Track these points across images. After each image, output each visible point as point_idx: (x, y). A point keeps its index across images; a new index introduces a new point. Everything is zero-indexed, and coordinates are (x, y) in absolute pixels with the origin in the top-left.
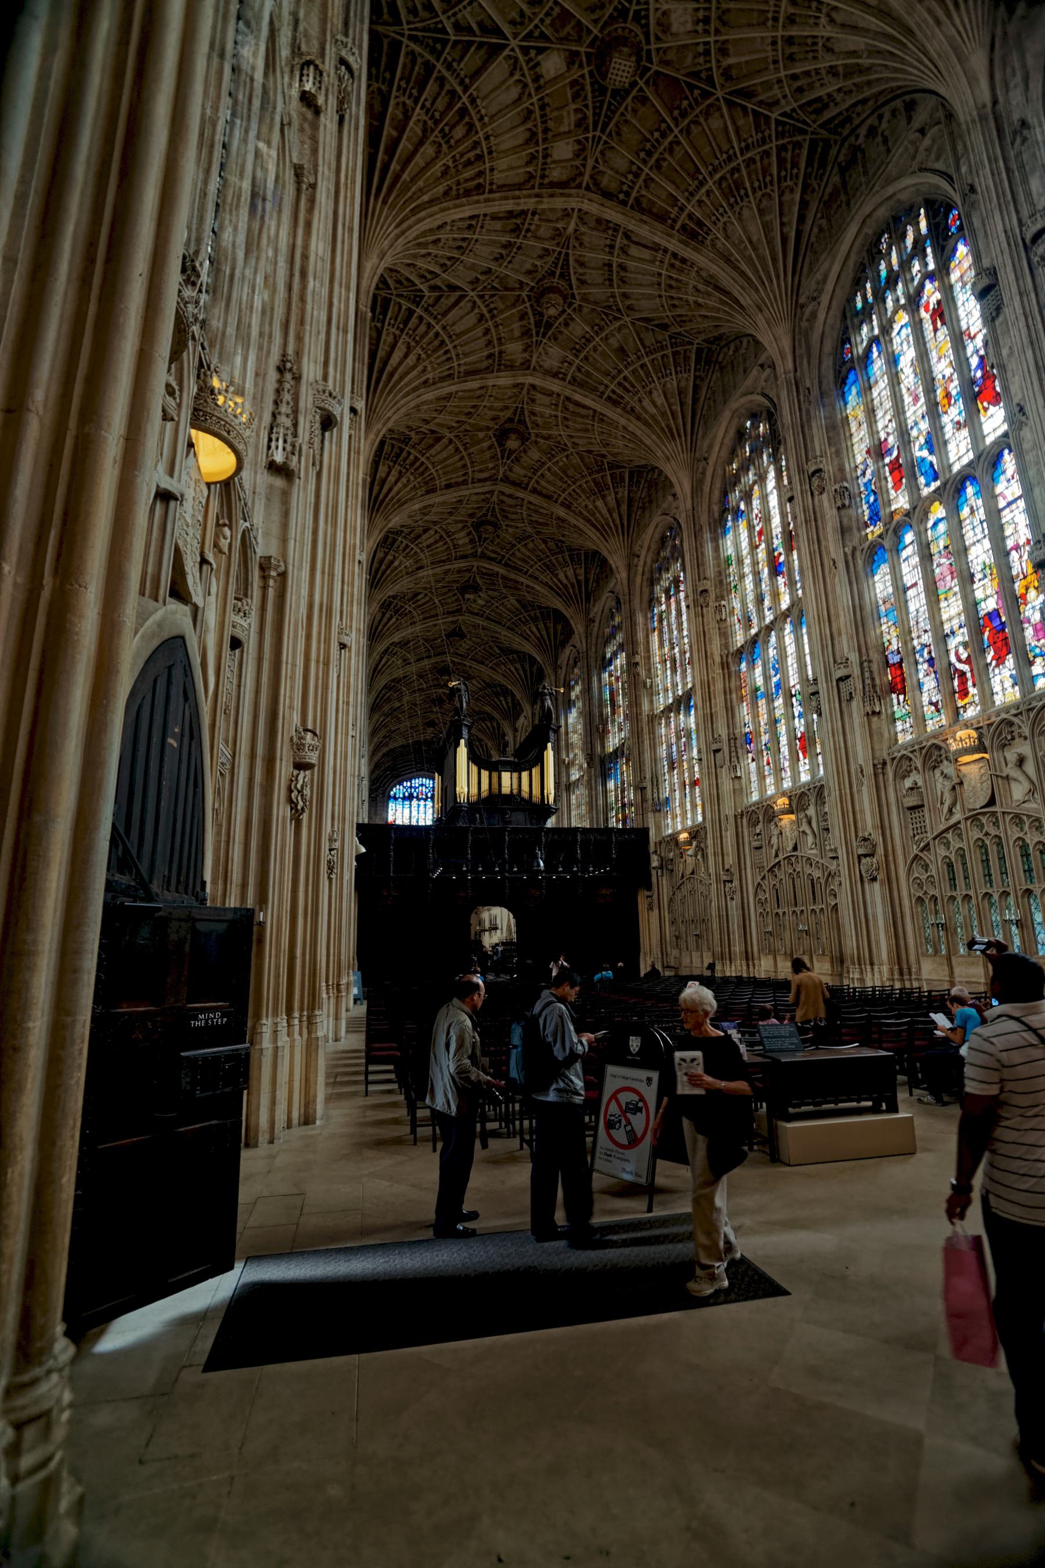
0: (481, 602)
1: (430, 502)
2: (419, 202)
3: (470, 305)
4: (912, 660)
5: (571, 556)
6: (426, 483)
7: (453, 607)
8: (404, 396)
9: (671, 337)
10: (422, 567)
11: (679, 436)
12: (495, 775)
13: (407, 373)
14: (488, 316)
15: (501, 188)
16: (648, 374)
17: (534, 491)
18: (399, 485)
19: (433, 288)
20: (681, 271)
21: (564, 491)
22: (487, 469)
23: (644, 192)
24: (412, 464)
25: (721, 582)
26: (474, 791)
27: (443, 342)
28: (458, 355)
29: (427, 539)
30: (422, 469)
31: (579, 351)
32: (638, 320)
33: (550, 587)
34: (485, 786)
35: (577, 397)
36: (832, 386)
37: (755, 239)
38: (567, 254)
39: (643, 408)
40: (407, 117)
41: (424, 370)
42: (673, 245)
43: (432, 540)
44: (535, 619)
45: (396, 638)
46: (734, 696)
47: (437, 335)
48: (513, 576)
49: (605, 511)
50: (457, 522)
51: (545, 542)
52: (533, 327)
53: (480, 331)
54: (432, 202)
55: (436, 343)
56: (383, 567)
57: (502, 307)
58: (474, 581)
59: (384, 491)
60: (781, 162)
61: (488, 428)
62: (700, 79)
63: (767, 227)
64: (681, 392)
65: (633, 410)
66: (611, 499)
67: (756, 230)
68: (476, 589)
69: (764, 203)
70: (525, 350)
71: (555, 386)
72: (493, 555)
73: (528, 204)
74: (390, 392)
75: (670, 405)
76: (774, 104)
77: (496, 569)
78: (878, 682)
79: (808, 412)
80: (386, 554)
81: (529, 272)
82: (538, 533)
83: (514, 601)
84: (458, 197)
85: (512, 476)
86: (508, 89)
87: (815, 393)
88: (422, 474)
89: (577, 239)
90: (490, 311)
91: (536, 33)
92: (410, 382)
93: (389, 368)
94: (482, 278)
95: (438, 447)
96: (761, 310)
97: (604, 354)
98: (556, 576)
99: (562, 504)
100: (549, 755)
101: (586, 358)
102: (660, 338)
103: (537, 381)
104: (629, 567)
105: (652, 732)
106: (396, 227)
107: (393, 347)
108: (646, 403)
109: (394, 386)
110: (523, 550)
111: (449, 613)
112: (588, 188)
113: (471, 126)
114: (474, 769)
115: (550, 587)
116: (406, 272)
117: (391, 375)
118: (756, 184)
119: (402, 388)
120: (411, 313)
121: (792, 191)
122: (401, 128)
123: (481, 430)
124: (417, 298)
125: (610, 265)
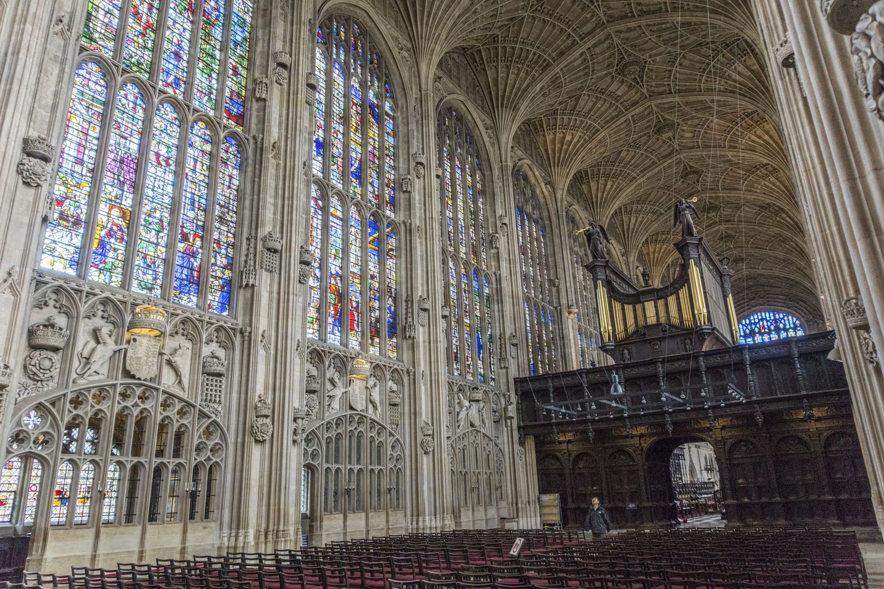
1: (550, 75)
5: (731, 52)
6: (537, 62)
7: (665, 150)
8: (445, 11)
10: (597, 131)
12: (639, 307)
17: (642, 13)
18: (512, 77)
22: (588, 21)
26: (620, 327)
29: (585, 103)
33: (732, 92)
34: (630, 321)
43: (590, 104)
44: (749, 128)
50: (602, 78)
51: (698, 53)
56: (558, 145)
58: (665, 120)
59: (501, 87)
68: (671, 126)
72: (661, 89)
85: (616, 13)
88: (527, 57)
114: (617, 306)
115: (732, 92)
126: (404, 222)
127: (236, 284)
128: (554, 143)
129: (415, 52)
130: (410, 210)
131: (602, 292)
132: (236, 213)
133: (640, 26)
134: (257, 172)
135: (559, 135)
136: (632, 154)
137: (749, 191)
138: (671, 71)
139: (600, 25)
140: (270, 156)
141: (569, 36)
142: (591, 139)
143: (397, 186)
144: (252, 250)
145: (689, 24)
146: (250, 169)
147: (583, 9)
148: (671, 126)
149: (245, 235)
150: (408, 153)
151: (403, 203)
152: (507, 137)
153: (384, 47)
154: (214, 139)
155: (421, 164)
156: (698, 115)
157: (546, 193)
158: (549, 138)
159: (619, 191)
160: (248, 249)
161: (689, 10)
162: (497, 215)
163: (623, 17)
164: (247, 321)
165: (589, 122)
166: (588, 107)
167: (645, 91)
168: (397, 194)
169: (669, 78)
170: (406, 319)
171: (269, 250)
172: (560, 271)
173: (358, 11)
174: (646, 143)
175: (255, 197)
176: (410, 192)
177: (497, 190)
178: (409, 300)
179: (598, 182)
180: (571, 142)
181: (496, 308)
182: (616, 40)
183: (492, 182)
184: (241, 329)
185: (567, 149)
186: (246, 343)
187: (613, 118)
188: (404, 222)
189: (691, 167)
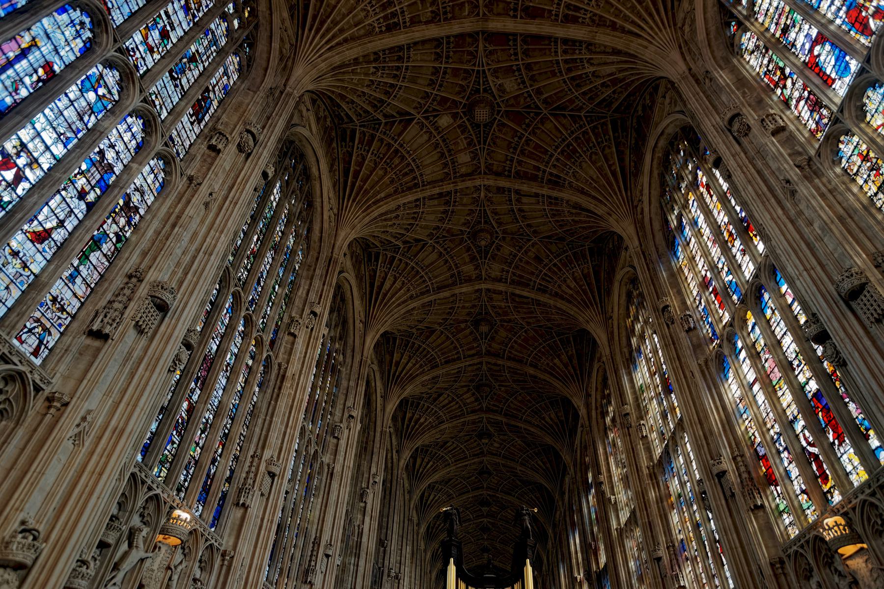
0: (496, 445)
2: (378, 197)
3: (431, 248)
4: (774, 451)
6: (430, 362)
8: (396, 307)
9: (568, 245)
10: (443, 422)
11: (592, 306)
13: (396, 293)
14: (444, 252)
15: (429, 183)
16: (560, 270)
17: (509, 358)
18: (410, 365)
19: (405, 242)
20: (556, 204)
21: (529, 356)
22: (472, 348)
23: (519, 168)
24: (418, 350)
25: (638, 406)
27: (418, 271)
28: (430, 278)
30: (425, 353)
31: (511, 264)
32: (544, 238)
35: (517, 292)
36: (666, 249)
37: (595, 177)
38: (485, 210)
39: (563, 291)
40: (364, 159)
41: (408, 290)
42: (545, 191)
43: (446, 401)
45: (436, 477)
46: (665, 503)
47: (413, 268)
48: (513, 423)
49: (561, 366)
50: (462, 387)
52: (476, 254)
53: (441, 262)
54: (386, 197)
55: (413, 273)
56: (412, 423)
57: (452, 246)
58: (487, 429)
59: (400, 369)
60: (597, 135)
61: (466, 321)
62: (532, 108)
63: (600, 170)
64: (586, 276)
65: (556, 292)
66: (564, 357)
67: (593, 172)
68: (490, 436)
69: (594, 157)
70: (476, 269)
71: (501, 287)
73: (449, 187)
74: (385, 306)
75: (580, 286)
76: (580, 109)
77: (499, 418)
78: (754, 475)
79: (654, 269)
80: (414, 415)
81: (464, 224)
82: (522, 389)
83: (519, 442)
84: (403, 191)
86: (421, 136)
87: (654, 256)
88: (425, 356)
89: (488, 200)
90: (445, 249)
91: (431, 109)
92: (400, 298)
93: (383, 291)
94: (434, 232)
95: (433, 337)
96: (610, 215)
97: (527, 263)
98: (544, 419)
99: (531, 365)
100: (529, 571)
101: (517, 267)
102: (561, 246)
103: (489, 286)
104: (588, 406)
105: (623, 546)
106: (363, 212)
107: (385, 279)
108: (564, 287)
109: (388, 301)
110: (515, 402)
111: (474, 455)
112: (485, 173)
113: (403, 158)
115: (541, 428)
116: (383, 236)
117: (385, 295)
118: (585, 149)
119: (394, 302)
120: (393, 258)
121: (609, 148)
122: (360, 164)
123: (462, 322)
124: (396, 249)
125: (513, 211)
126: (328, 465)
127: (230, 499)
128: (410, 420)
129: (366, 324)
130: (335, 455)
131: (452, 570)
132: (247, 427)
133: (504, 366)
134: (275, 395)
135: (416, 416)
136: (455, 445)
137: (520, 499)
138: (508, 400)
139: (479, 354)
140: (287, 384)
141: (458, 352)
142: (437, 426)
143: (329, 430)
144: (253, 469)
145: (535, 377)
146: (269, 391)
147: (474, 340)
148: (490, 436)
149: (251, 453)
150: (345, 405)
151: (332, 447)
152: (391, 407)
153: (351, 314)
154: (257, 357)
155: (353, 417)
156: (510, 434)
157: (395, 460)
158: (408, 415)
159: (435, 471)
160: (250, 467)
161: (540, 369)
162: (372, 473)
163: (496, 355)
164: (231, 543)
165: (441, 414)
166: (444, 403)
167: (484, 406)
168: (328, 438)
169: (505, 404)
170: (310, 561)
171: (269, 473)
172: (389, 532)
173: (347, 284)
174: (466, 442)
175: (268, 418)
176: (338, 439)
177: (375, 450)
178: (317, 542)
179: (423, 459)
180: (423, 424)
181: (353, 562)
182: (484, 367)
183: (374, 441)
184: (225, 551)
185: (418, 429)
186: (225, 568)
187: (456, 417)
188: (328, 465)
189: (487, 468)
